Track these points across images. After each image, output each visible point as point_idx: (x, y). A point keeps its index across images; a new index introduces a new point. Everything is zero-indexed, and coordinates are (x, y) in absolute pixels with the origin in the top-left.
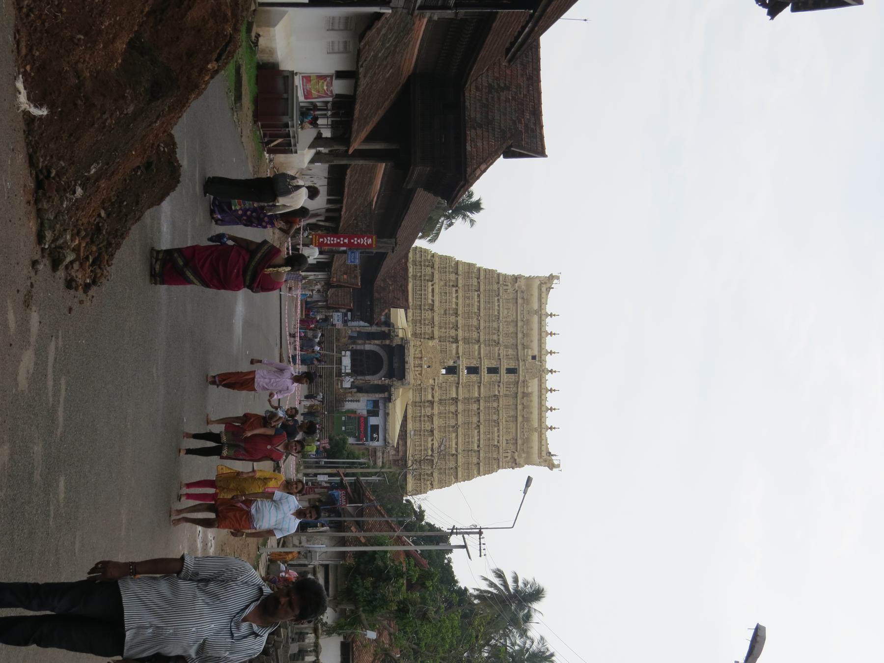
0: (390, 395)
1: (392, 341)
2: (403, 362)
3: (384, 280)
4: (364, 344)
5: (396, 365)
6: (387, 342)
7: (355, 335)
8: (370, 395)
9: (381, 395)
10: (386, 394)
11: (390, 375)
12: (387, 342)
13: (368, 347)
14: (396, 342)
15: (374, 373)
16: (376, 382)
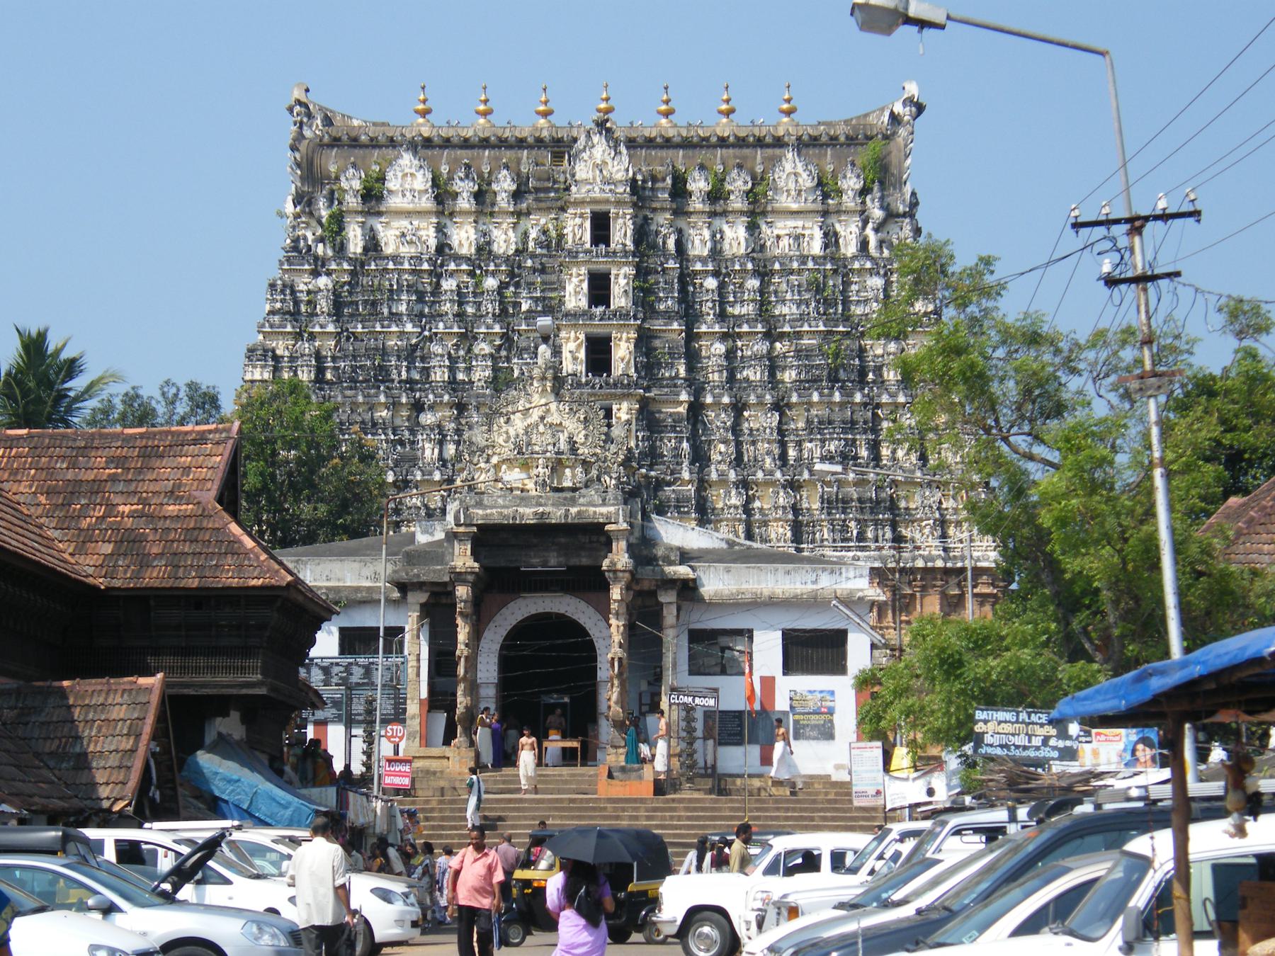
0: (670, 583)
1: (458, 577)
2: (543, 532)
3: (85, 540)
4: (473, 688)
5: (555, 561)
6: (462, 591)
7: (441, 718)
8: (668, 660)
9: (670, 615)
10: (668, 598)
11: (591, 583)
12: (462, 591)
13: (488, 671)
14: (463, 559)
15: (586, 650)
16: (617, 638)
